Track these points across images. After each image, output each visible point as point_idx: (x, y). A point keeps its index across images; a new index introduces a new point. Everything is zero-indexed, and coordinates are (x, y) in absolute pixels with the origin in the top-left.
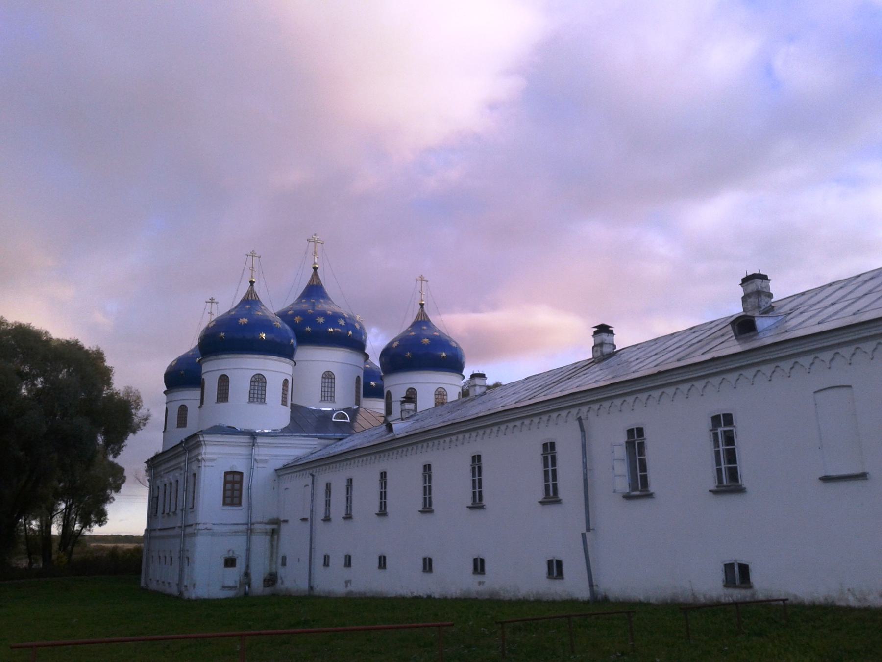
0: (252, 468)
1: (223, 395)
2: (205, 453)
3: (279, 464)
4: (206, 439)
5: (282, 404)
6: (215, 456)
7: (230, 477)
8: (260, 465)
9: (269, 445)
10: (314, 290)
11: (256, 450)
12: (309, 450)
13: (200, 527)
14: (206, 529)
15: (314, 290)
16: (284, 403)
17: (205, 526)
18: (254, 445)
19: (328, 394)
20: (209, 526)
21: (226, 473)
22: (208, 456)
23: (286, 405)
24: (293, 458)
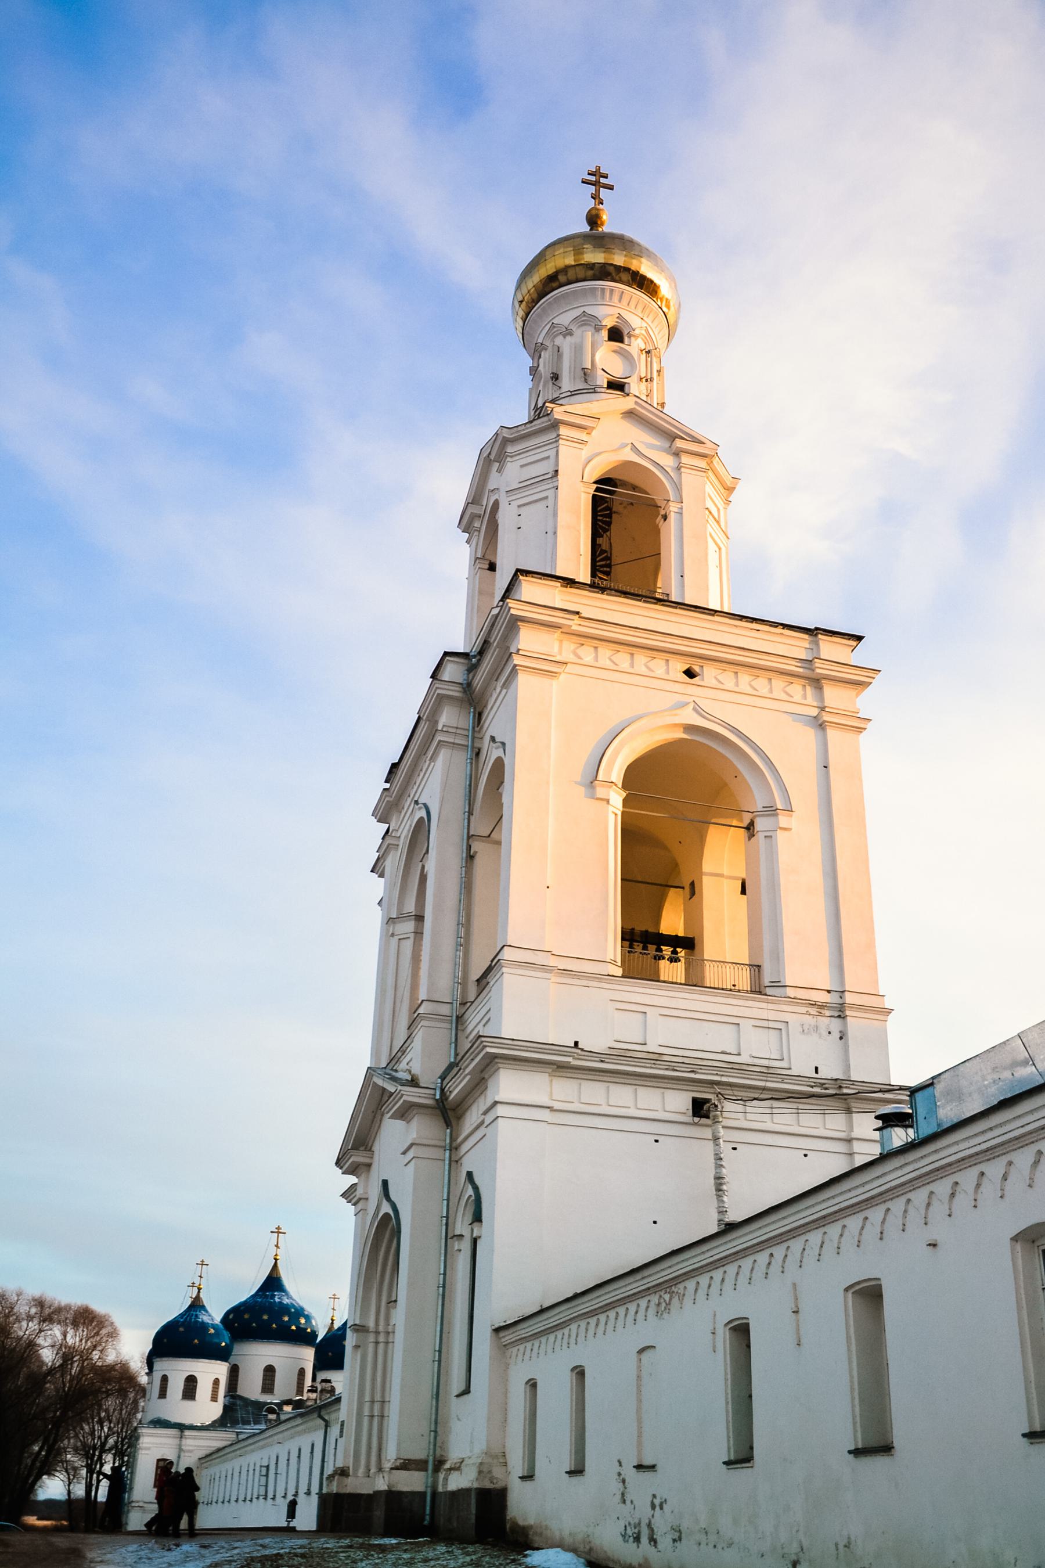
0: (179, 1457)
1: (163, 1394)
2: (142, 1443)
3: (202, 1453)
4: (143, 1431)
5: (212, 1400)
6: (151, 1445)
7: (161, 1464)
8: (187, 1454)
9: (195, 1438)
10: (273, 1283)
11: (184, 1441)
12: (230, 1443)
13: (133, 1504)
14: (138, 1506)
15: (273, 1283)
16: (214, 1398)
17: (137, 1504)
18: (181, 1437)
19: (268, 1386)
20: (141, 1504)
21: (158, 1460)
22: (144, 1445)
23: (216, 1401)
24: (214, 1449)
